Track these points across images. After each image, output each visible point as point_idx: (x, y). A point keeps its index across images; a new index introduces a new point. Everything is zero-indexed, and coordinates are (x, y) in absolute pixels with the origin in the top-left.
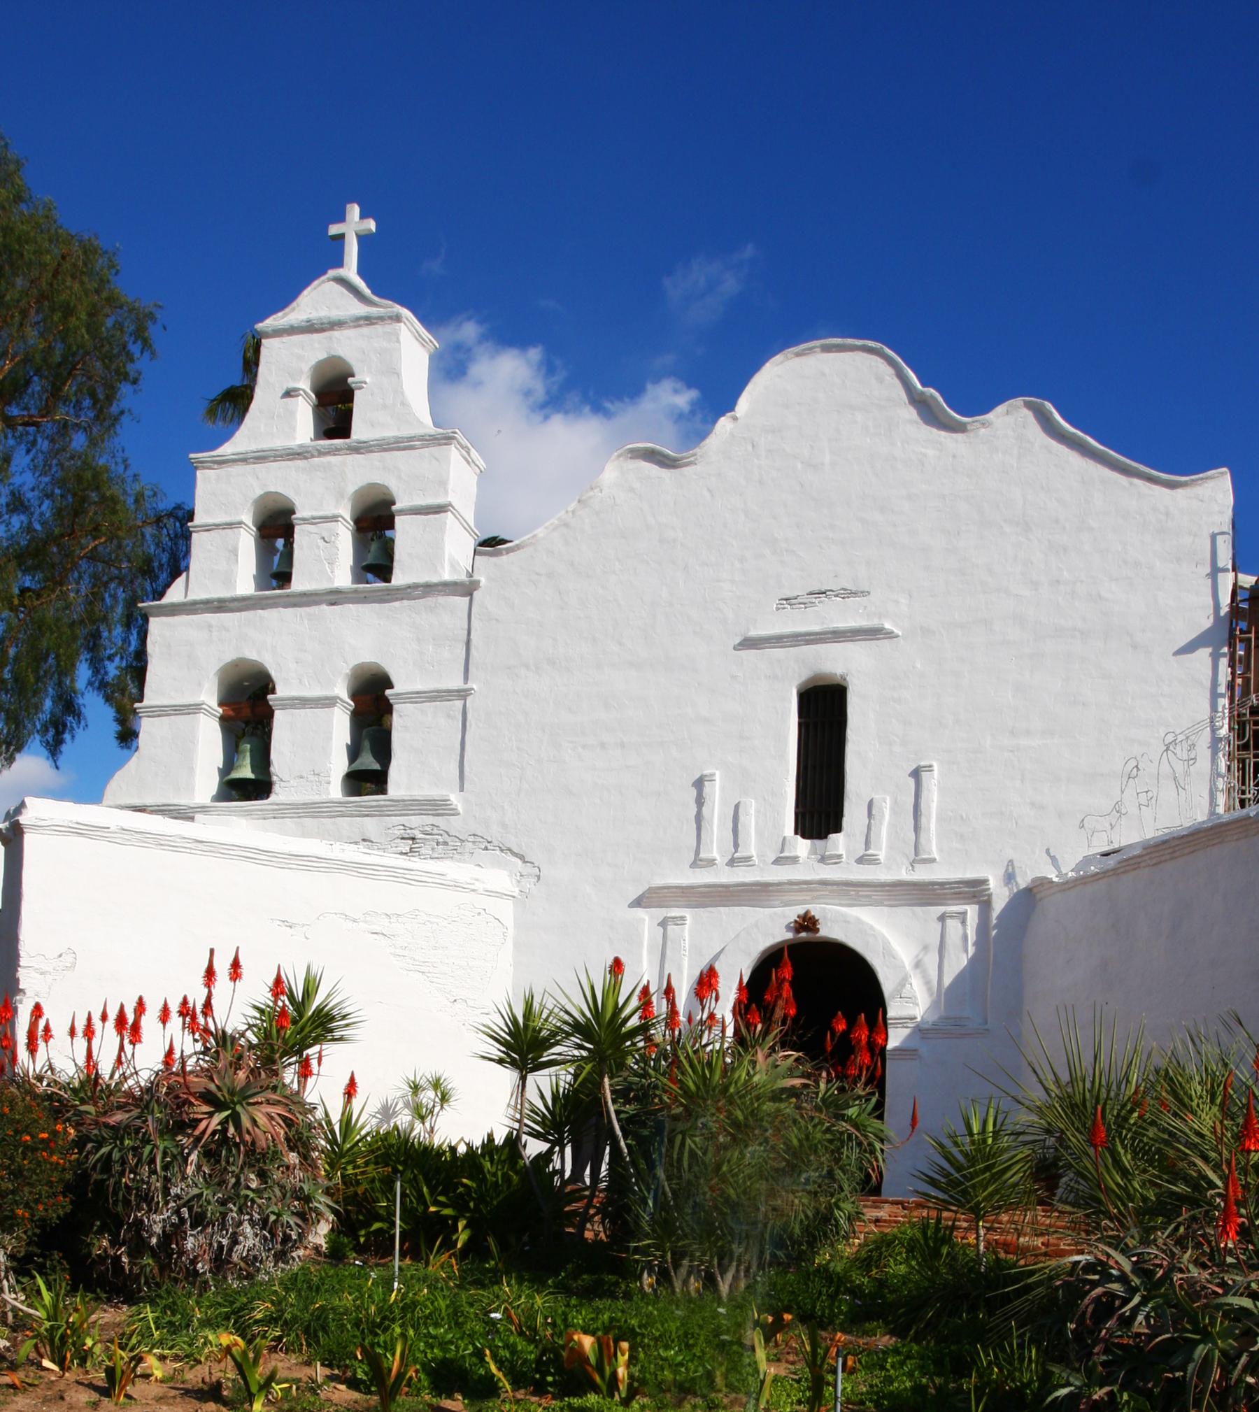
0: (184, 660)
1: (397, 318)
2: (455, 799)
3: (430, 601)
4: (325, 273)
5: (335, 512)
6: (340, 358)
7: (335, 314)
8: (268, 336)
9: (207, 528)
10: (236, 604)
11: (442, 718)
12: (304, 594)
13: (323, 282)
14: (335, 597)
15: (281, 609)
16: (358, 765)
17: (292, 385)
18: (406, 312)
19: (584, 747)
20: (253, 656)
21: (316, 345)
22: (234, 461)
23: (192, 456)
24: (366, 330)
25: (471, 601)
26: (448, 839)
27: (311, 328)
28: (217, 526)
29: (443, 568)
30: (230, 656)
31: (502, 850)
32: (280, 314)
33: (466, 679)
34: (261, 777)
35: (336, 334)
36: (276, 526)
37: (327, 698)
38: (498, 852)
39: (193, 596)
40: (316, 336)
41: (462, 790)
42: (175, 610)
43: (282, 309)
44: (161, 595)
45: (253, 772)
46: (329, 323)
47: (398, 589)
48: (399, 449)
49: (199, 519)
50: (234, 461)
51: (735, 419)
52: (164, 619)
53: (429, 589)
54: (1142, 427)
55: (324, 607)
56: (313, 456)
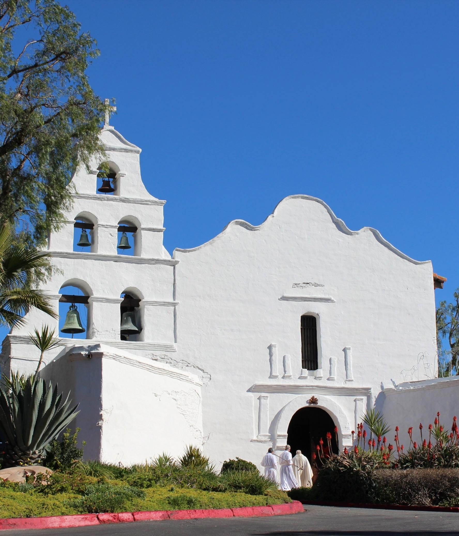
2: (175, 345)
3: (158, 266)
25: (174, 268)
26: (172, 361)
41: (176, 342)
51: (273, 217)
54: (405, 242)
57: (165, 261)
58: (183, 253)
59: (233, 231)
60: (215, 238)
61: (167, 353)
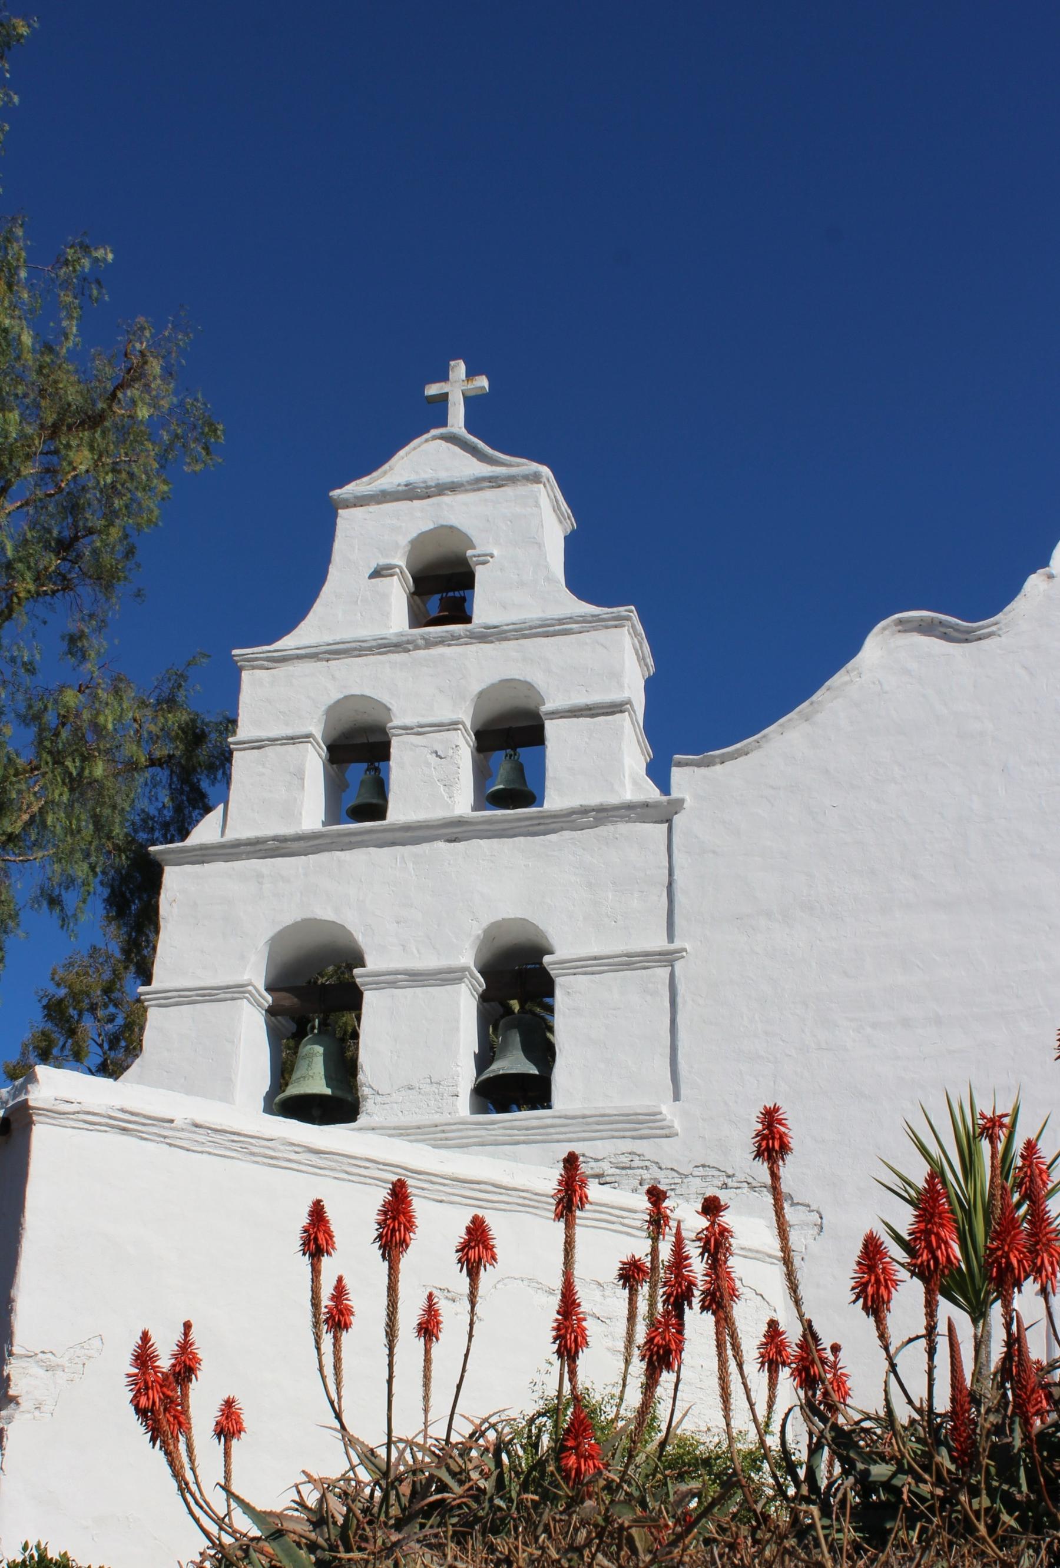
0: (218, 929)
1: (536, 478)
2: (668, 1110)
3: (605, 830)
4: (428, 431)
5: (454, 717)
6: (451, 528)
7: (445, 476)
8: (347, 504)
9: (258, 745)
10: (302, 844)
11: (640, 997)
12: (407, 828)
13: (427, 441)
14: (454, 831)
15: (373, 850)
16: (501, 1066)
17: (383, 561)
18: (545, 471)
19: (874, 1026)
20: (326, 913)
21: (419, 514)
22: (299, 657)
23: (235, 652)
24: (490, 494)
25: (670, 830)
27: (411, 493)
28: (273, 741)
29: (623, 785)
30: (290, 915)
31: (753, 1188)
32: (365, 479)
33: (671, 938)
34: (339, 1094)
35: (447, 499)
36: (359, 754)
37: (450, 971)
38: (746, 1189)
39: (231, 835)
40: (417, 503)
41: (677, 1097)
42: (205, 855)
43: (368, 472)
44: (184, 834)
45: (328, 1086)
46: (438, 485)
47: (555, 816)
48: (547, 635)
49: (245, 730)
50: (299, 657)
51: (1051, 577)
52: (188, 868)
53: (602, 815)
55: (441, 845)
56: (417, 648)
57: (630, 807)
58: (703, 771)
59: (892, 658)
60: (819, 696)
61: (642, 1147)
